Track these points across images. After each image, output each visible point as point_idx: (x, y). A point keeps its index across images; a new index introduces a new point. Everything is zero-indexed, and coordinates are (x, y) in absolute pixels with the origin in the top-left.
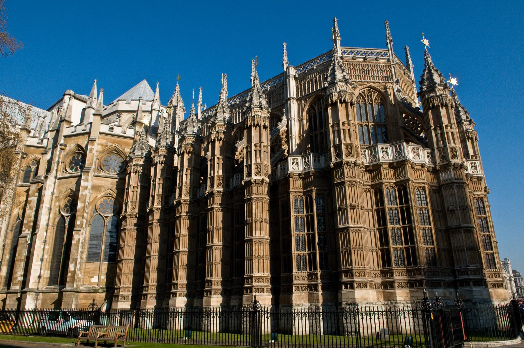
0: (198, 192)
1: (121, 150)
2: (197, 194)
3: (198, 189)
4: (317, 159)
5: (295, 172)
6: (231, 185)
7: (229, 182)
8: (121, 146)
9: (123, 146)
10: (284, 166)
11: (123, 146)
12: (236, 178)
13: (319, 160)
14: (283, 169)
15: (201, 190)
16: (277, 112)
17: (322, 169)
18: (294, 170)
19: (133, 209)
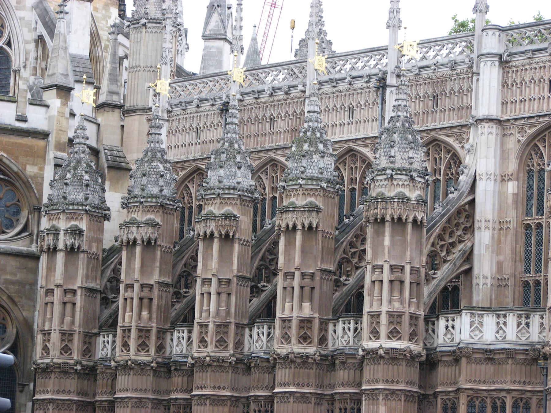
0: (247, 336)
1: (16, 169)
2: (243, 343)
3: (247, 330)
4: (523, 321)
5: (476, 347)
6: (330, 338)
7: (326, 330)
8: (16, 159)
9: (22, 159)
10: (453, 320)
11: (22, 159)
12: (344, 329)
13: (528, 325)
14: (450, 328)
15: (255, 337)
16: (450, 140)
17: (532, 345)
18: (472, 341)
19: (66, 349)
